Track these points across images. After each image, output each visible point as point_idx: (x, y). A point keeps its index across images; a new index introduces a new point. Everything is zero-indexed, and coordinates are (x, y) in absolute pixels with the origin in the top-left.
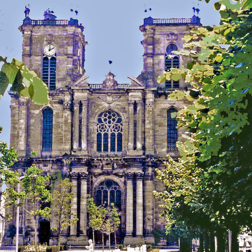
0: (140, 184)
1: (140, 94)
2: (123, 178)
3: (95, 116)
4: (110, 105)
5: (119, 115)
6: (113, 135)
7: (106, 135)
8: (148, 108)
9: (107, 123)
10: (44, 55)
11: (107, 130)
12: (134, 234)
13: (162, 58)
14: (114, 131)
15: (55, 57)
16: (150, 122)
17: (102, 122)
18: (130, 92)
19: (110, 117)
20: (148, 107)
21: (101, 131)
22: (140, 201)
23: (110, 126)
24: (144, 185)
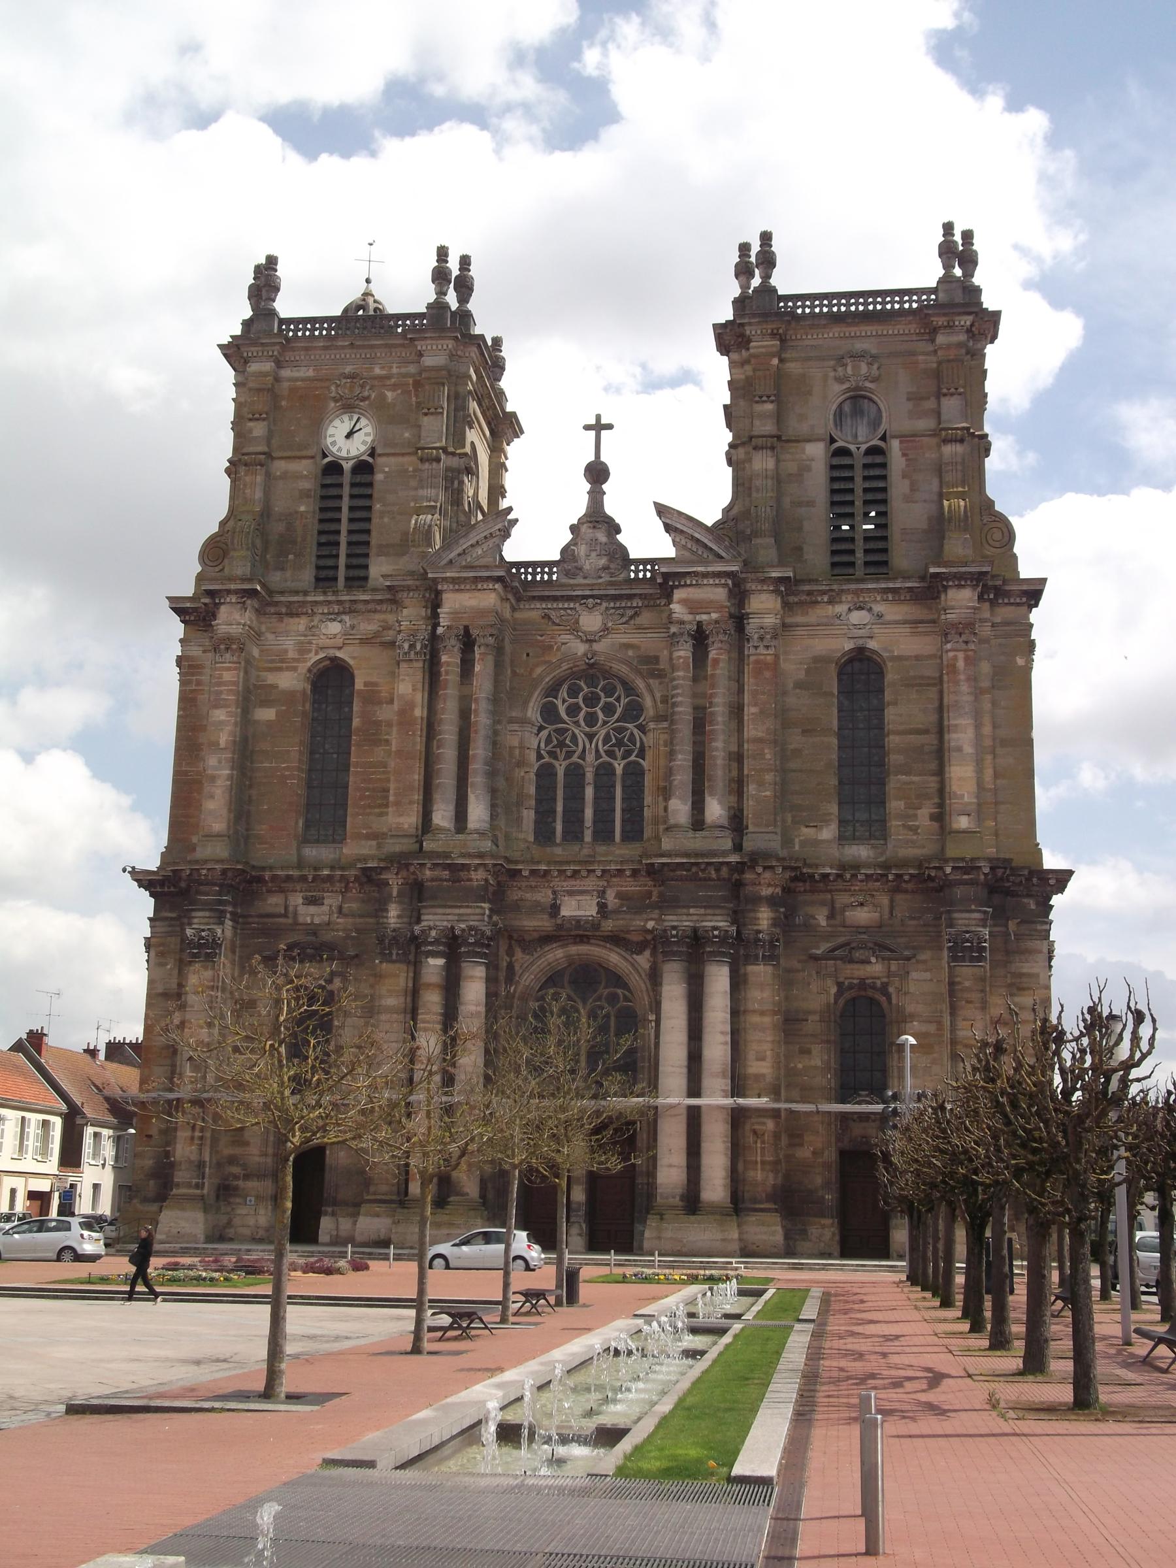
0: (719, 979)
1: (719, 594)
2: (647, 953)
3: (530, 695)
4: (596, 647)
5: (629, 689)
6: (604, 773)
7: (575, 775)
8: (757, 653)
9: (582, 723)
10: (325, 456)
12: (692, 1202)
13: (816, 451)
14: (610, 754)
15: (370, 460)
16: (762, 712)
19: (592, 700)
20: (756, 647)
21: (556, 758)
22: (716, 1050)
23: (590, 737)
24: (738, 984)
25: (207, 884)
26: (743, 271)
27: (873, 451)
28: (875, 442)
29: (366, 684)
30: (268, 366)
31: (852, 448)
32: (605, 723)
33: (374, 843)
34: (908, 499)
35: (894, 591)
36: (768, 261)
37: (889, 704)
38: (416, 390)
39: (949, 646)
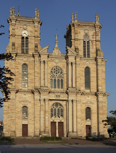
6: (59, 80)
11: (55, 77)
14: (59, 78)
17: (53, 73)
27: (88, 42)
28: (88, 41)
30: (14, 22)
34: (92, 48)
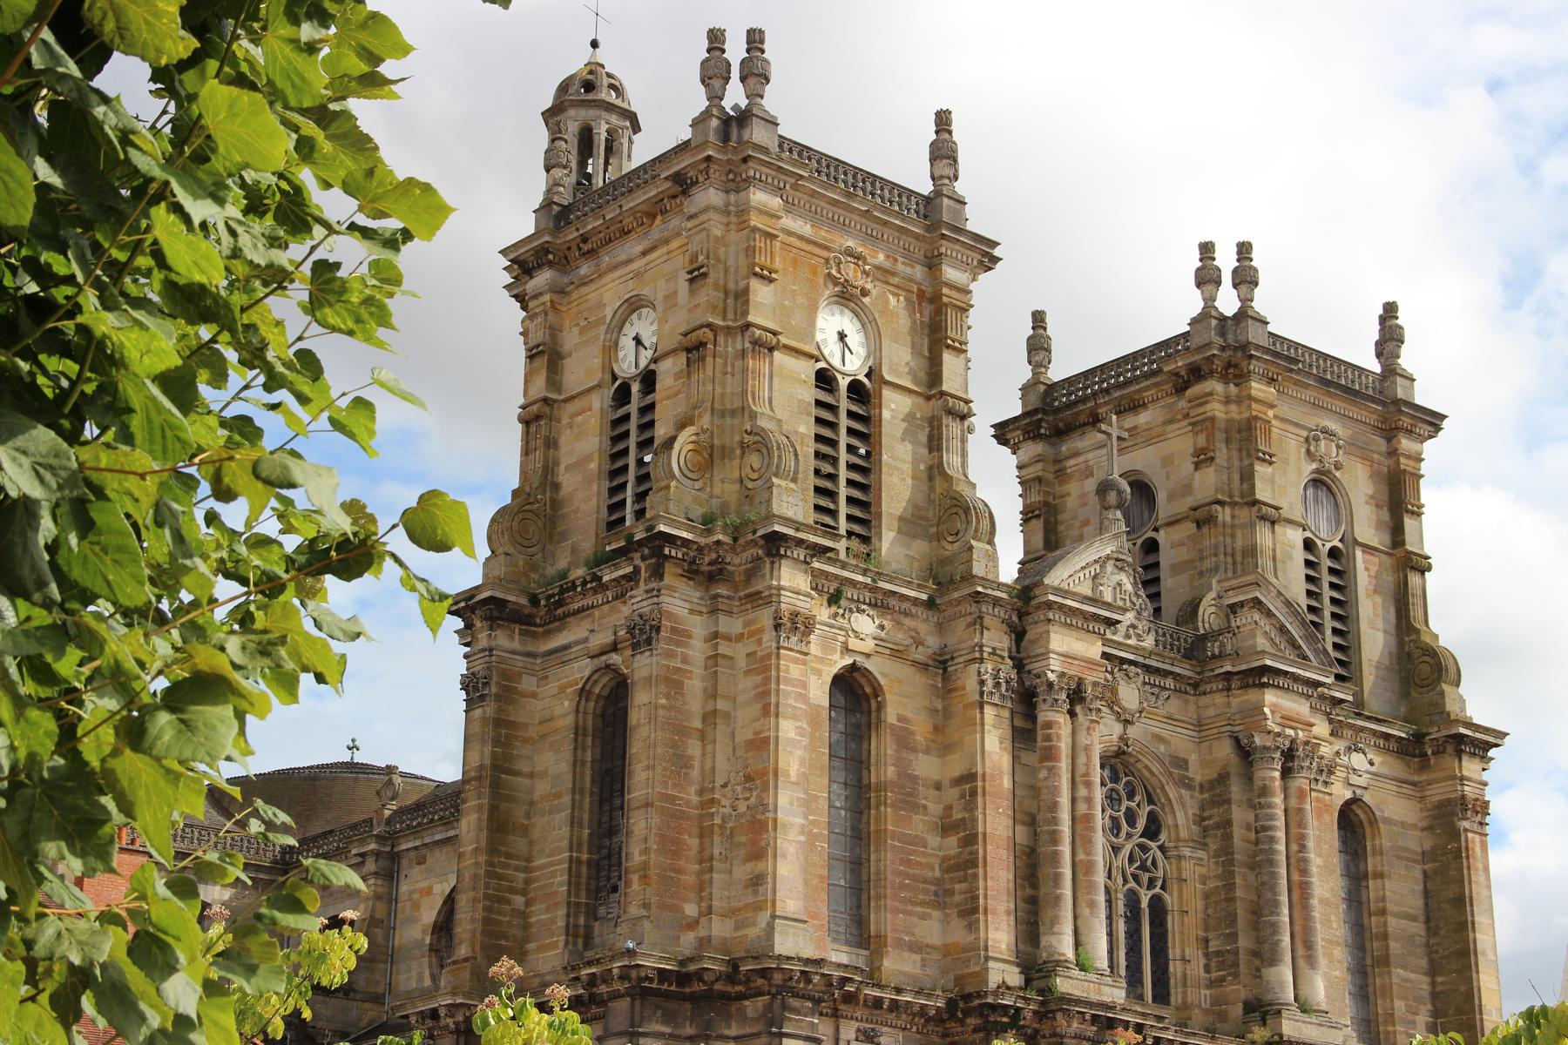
13: (1295, 537)
18: (1273, 686)
25: (803, 997)
26: (1207, 278)
29: (900, 718)
31: (1319, 543)
32: (1129, 836)
33: (917, 957)
35: (1387, 736)
36: (1245, 278)
37: (1380, 876)
38: (920, 304)
39: (1466, 824)
